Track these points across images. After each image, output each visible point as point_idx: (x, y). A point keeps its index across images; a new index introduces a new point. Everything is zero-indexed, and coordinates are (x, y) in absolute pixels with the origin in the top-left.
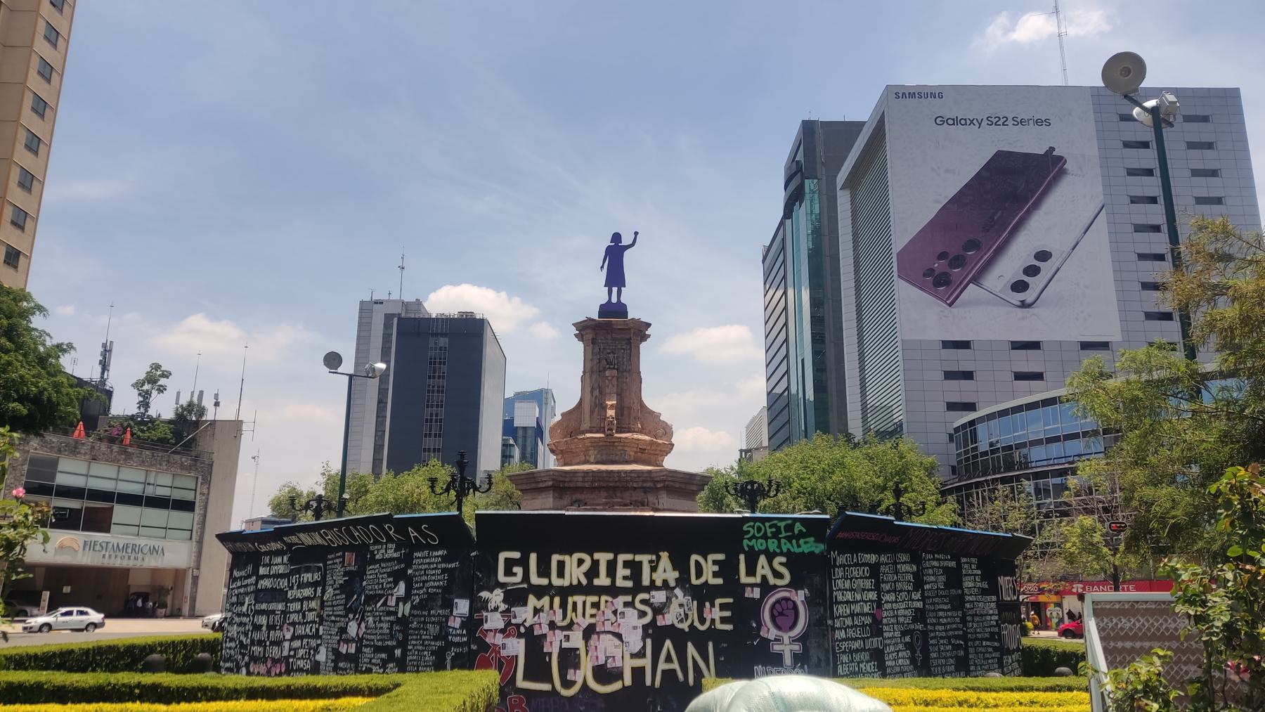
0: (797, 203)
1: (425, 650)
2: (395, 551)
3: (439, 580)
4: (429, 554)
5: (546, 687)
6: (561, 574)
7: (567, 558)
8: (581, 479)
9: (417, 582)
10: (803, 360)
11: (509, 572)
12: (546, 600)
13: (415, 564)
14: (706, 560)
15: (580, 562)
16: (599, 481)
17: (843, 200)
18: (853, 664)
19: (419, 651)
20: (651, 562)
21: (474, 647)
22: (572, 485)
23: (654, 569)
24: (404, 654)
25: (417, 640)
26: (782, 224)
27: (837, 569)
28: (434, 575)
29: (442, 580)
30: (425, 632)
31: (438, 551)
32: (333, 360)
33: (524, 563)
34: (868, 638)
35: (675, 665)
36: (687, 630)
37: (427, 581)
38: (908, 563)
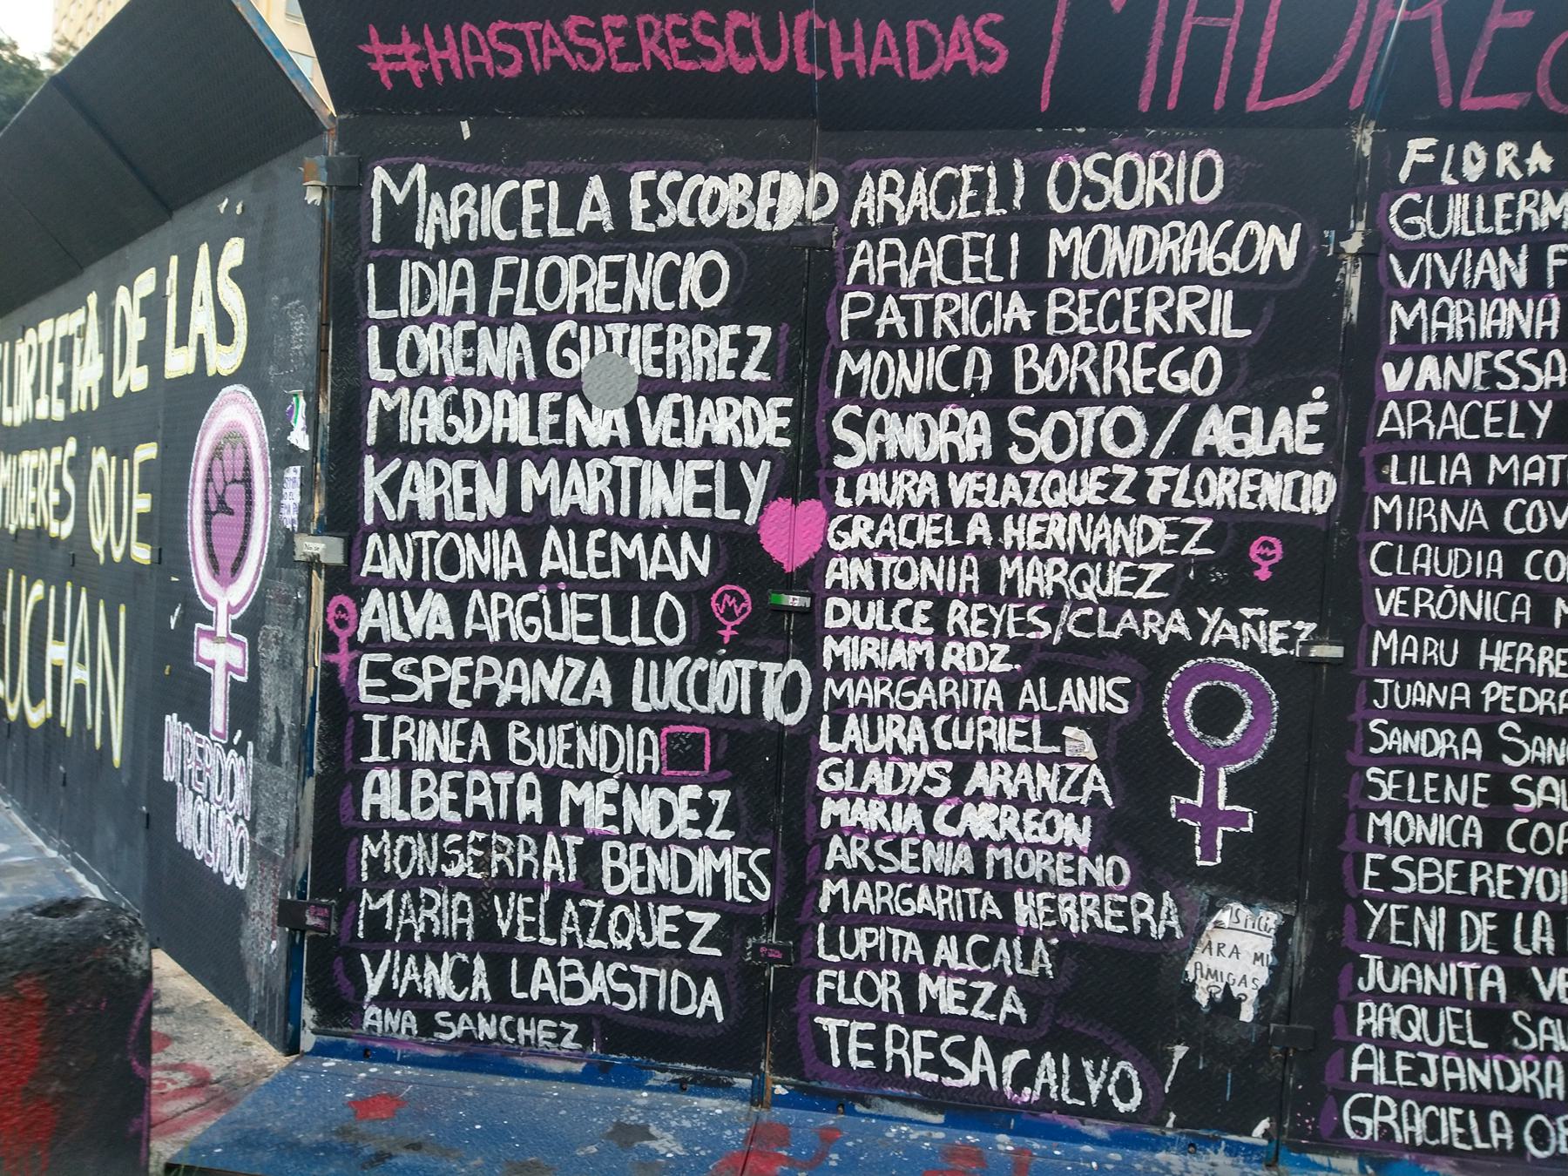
18: (504, 778)
27: (410, 272)
34: (675, 655)
38: (1189, 213)
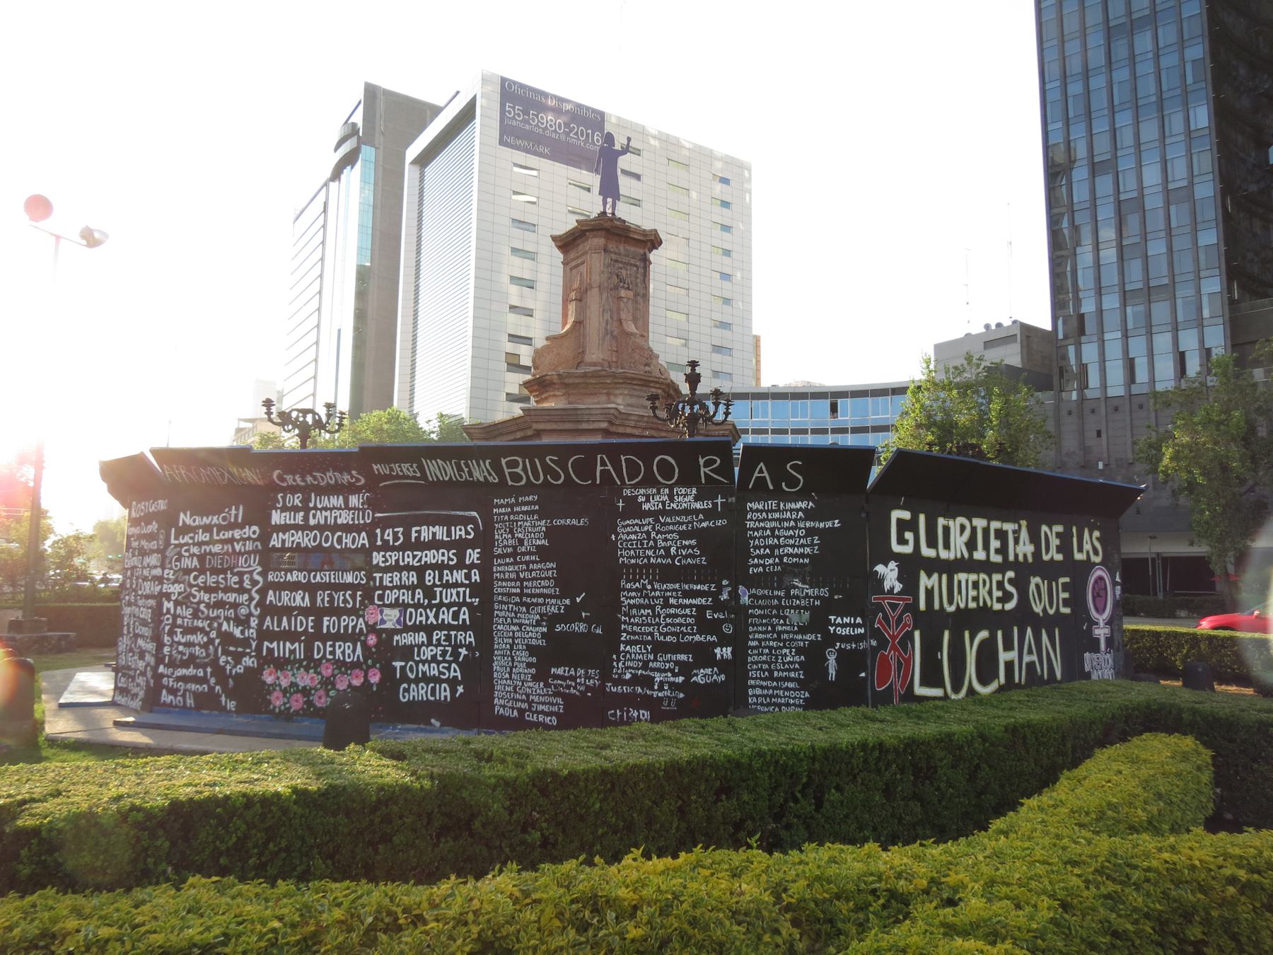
0: (349, 168)
1: (785, 647)
2: (697, 499)
3: (803, 546)
4: (778, 505)
5: (937, 692)
6: (947, 546)
7: (951, 523)
8: (632, 424)
9: (756, 547)
10: (339, 331)
11: (902, 541)
12: (935, 576)
13: (751, 520)
14: (1051, 530)
15: (963, 528)
16: (652, 428)
17: (410, 173)
19: (770, 648)
20: (1015, 532)
21: (874, 643)
22: (621, 430)
23: (1017, 541)
24: (741, 651)
25: (766, 632)
26: (326, 184)
28: (791, 537)
29: (808, 546)
30: (782, 621)
31: (795, 501)
32: (39, 207)
33: (911, 525)
35: (1034, 658)
36: (1041, 614)
37: (779, 546)
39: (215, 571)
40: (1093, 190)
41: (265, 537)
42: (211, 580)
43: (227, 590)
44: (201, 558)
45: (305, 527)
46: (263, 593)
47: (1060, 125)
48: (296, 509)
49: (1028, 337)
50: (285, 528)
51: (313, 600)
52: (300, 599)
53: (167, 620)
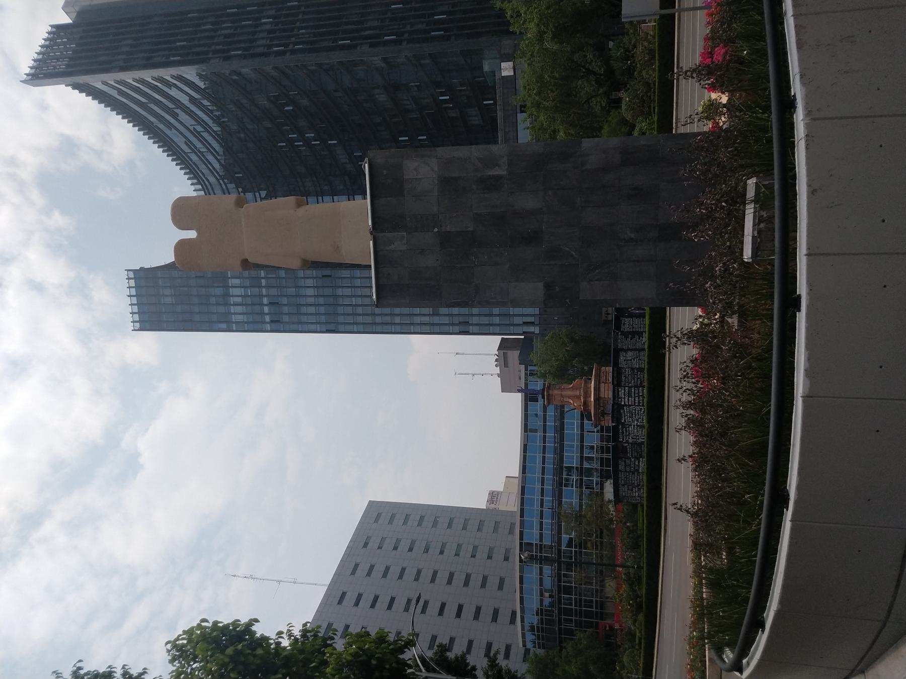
39: (632, 415)
40: (445, 315)
41: (626, 406)
42: (634, 415)
43: (635, 412)
44: (630, 417)
45: (624, 398)
46: (636, 406)
47: (412, 327)
48: (621, 400)
49: (505, 348)
50: (625, 402)
51: (637, 397)
52: (637, 399)
53: (641, 424)
